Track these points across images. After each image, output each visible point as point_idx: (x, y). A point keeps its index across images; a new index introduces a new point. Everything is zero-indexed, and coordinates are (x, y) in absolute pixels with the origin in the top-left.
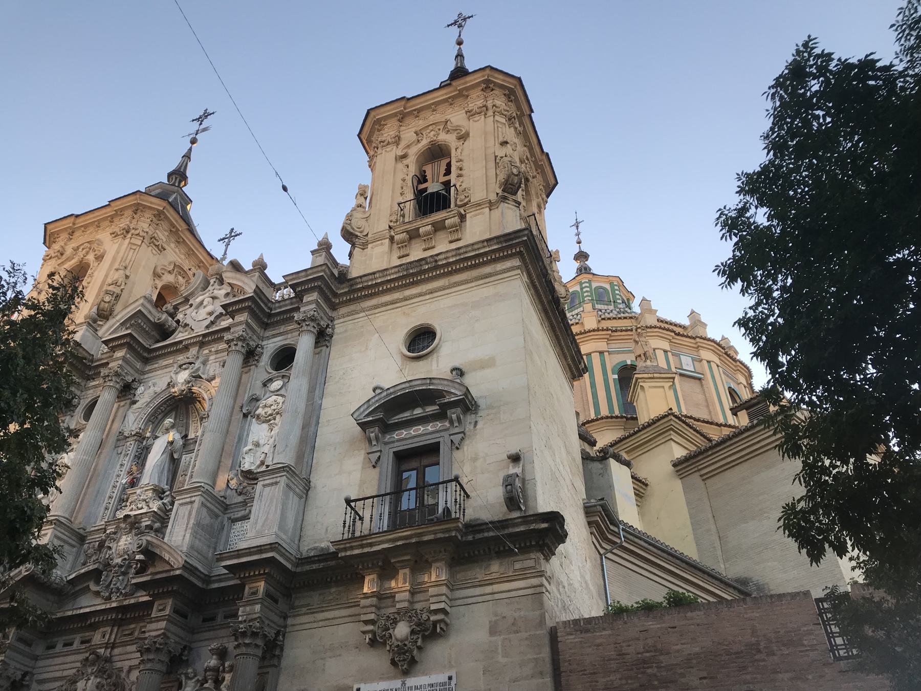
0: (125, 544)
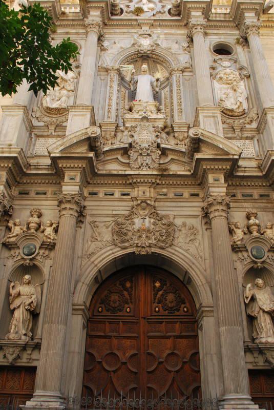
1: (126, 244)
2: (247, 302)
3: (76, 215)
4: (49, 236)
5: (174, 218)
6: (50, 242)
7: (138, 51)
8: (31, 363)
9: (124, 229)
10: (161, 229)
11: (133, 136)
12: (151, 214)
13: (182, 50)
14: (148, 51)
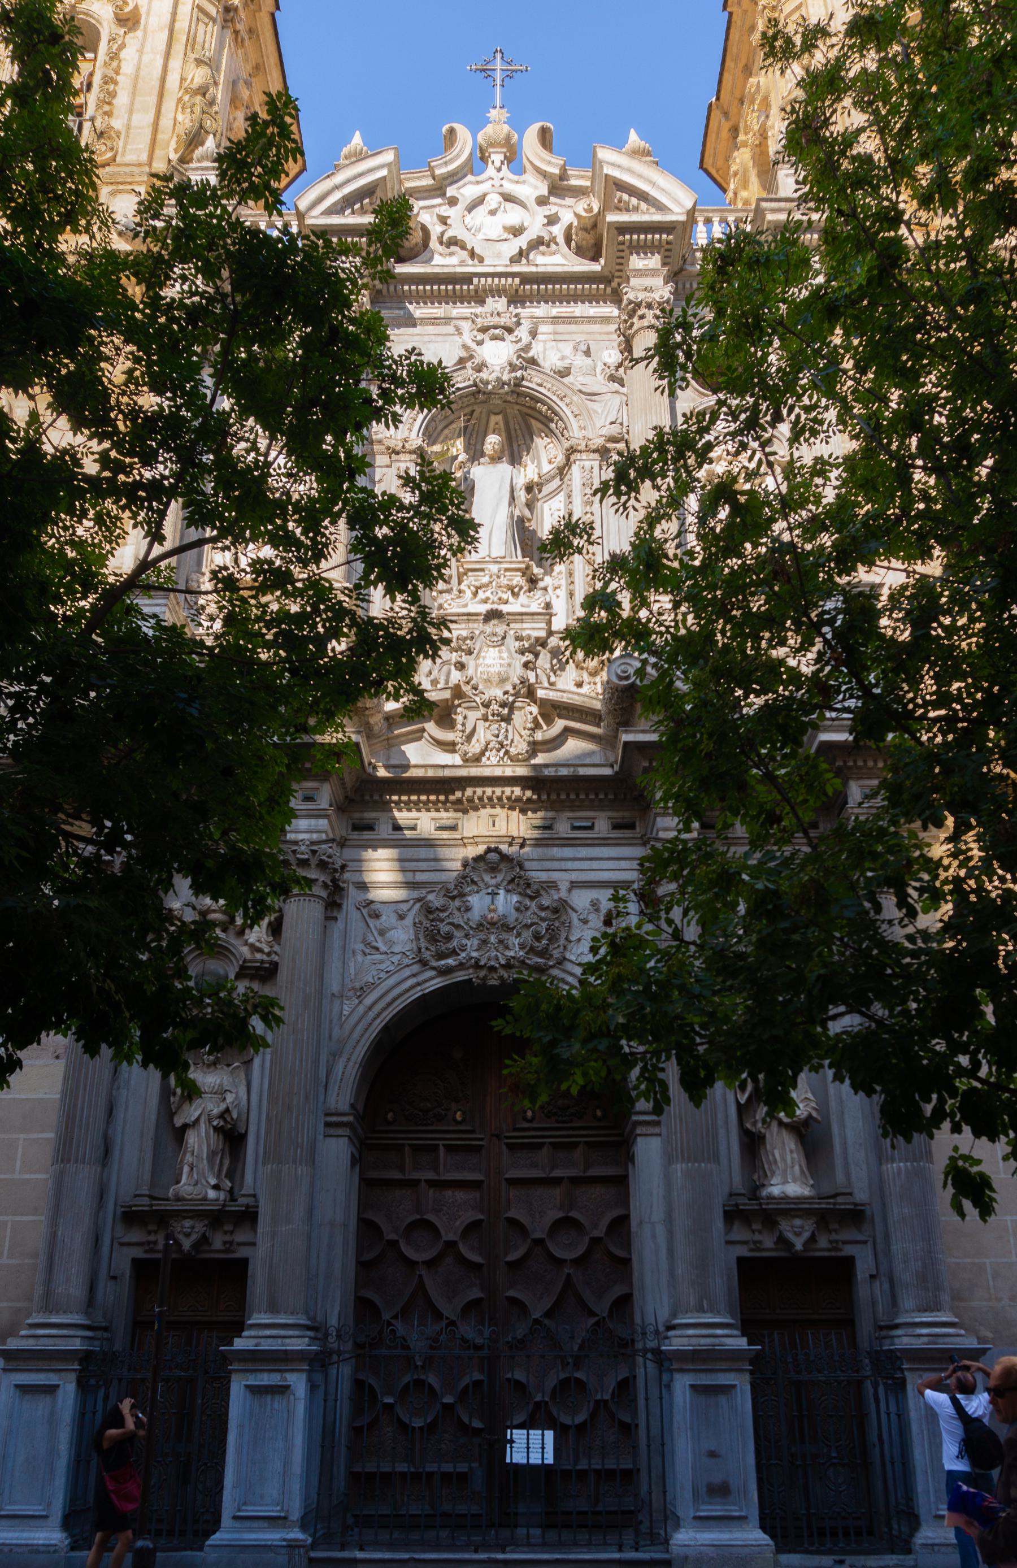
0: (501, 665)
1: (451, 961)
2: (742, 1102)
3: (324, 894)
4: (258, 944)
5: (570, 890)
6: (262, 962)
7: (475, 385)
8: (234, 1252)
9: (442, 921)
11: (461, 666)
12: (512, 881)
13: (600, 378)
14: (504, 383)
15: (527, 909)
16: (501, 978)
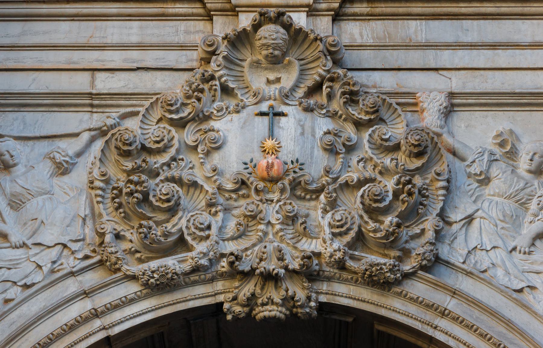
10: (369, 173)
12: (316, 89)
15: (350, 149)
16: (289, 300)
